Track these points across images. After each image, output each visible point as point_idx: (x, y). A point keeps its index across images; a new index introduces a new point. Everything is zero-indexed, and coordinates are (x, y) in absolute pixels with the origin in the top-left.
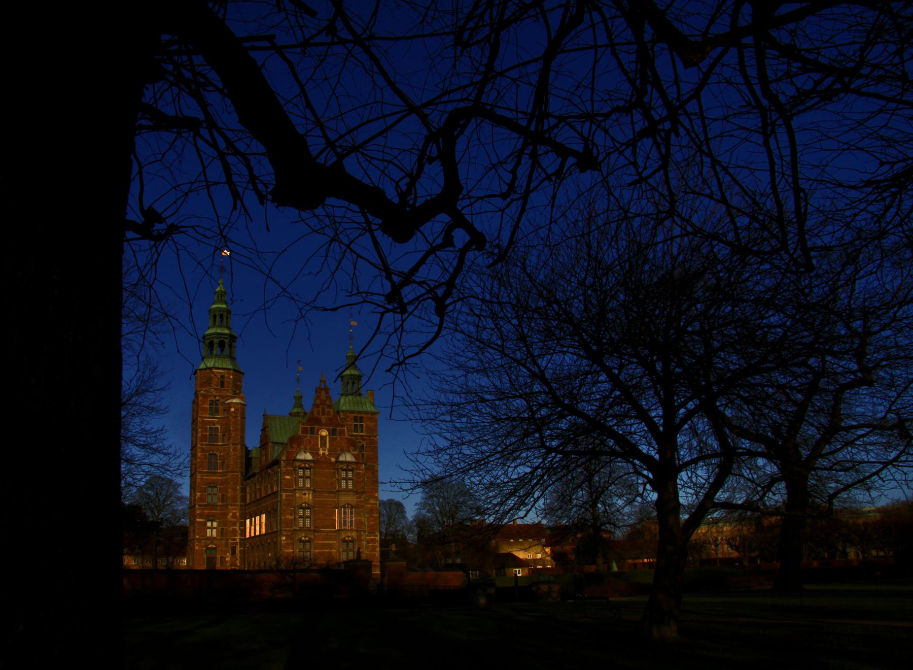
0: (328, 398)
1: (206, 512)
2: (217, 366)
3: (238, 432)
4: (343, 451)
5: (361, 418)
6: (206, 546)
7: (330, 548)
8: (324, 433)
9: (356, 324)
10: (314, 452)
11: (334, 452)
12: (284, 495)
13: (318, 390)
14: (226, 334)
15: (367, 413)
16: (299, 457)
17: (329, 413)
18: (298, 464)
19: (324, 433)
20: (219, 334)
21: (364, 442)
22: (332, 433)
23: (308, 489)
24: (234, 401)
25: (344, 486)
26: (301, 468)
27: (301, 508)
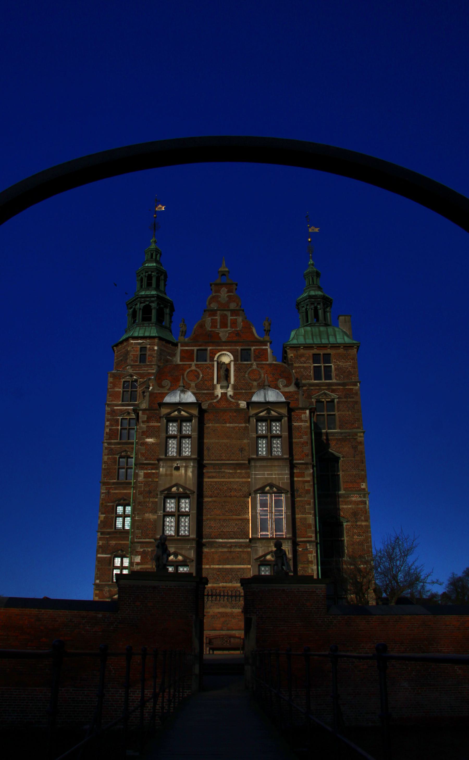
1: (113, 543)
2: (136, 334)
4: (262, 386)
8: (227, 358)
9: (317, 230)
10: (203, 390)
11: (244, 389)
12: (141, 473)
14: (153, 296)
15: (335, 346)
16: (168, 399)
17: (234, 323)
18: (164, 411)
19: (227, 358)
21: (334, 395)
22: (242, 357)
23: (186, 459)
25: (263, 451)
26: (174, 420)
27: (170, 496)
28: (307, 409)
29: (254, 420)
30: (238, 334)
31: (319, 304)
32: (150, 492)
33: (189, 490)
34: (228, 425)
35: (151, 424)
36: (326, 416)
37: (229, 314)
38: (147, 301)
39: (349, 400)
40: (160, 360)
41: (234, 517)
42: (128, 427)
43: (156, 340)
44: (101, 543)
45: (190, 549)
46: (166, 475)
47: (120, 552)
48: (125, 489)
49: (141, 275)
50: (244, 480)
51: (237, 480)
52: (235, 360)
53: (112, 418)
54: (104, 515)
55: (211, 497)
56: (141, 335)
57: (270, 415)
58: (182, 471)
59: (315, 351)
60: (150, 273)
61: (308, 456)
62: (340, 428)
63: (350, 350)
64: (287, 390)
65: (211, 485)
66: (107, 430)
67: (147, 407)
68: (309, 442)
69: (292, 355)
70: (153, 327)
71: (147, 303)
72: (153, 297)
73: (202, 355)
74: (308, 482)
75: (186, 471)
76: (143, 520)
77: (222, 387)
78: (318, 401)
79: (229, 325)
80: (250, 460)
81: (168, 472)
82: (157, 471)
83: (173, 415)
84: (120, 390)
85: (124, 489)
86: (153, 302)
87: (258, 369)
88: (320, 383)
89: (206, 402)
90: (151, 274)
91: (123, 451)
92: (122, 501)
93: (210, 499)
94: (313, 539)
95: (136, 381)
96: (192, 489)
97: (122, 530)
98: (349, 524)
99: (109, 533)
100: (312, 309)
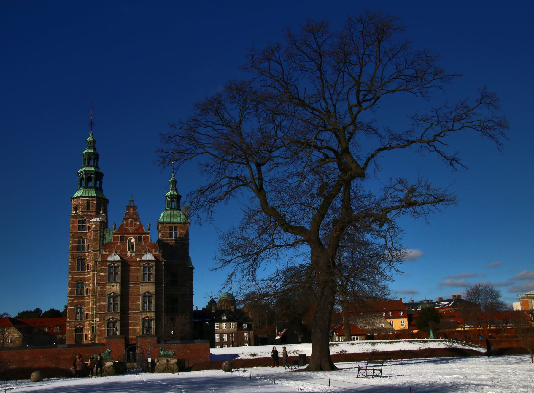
0: (135, 213)
1: (76, 301)
2: (84, 195)
3: (98, 242)
4: (146, 252)
5: (176, 227)
6: (75, 327)
7: (136, 326)
8: (133, 240)
12: (99, 287)
13: (129, 208)
14: (92, 171)
16: (110, 258)
17: (135, 224)
22: (139, 239)
24: (95, 219)
30: (137, 229)
32: (102, 294)
44: (69, 302)
48: (81, 275)
52: (136, 241)
56: (87, 195)
58: (115, 287)
59: (171, 225)
64: (155, 253)
66: (71, 246)
73: (122, 239)
95: (85, 220)
99: (73, 297)
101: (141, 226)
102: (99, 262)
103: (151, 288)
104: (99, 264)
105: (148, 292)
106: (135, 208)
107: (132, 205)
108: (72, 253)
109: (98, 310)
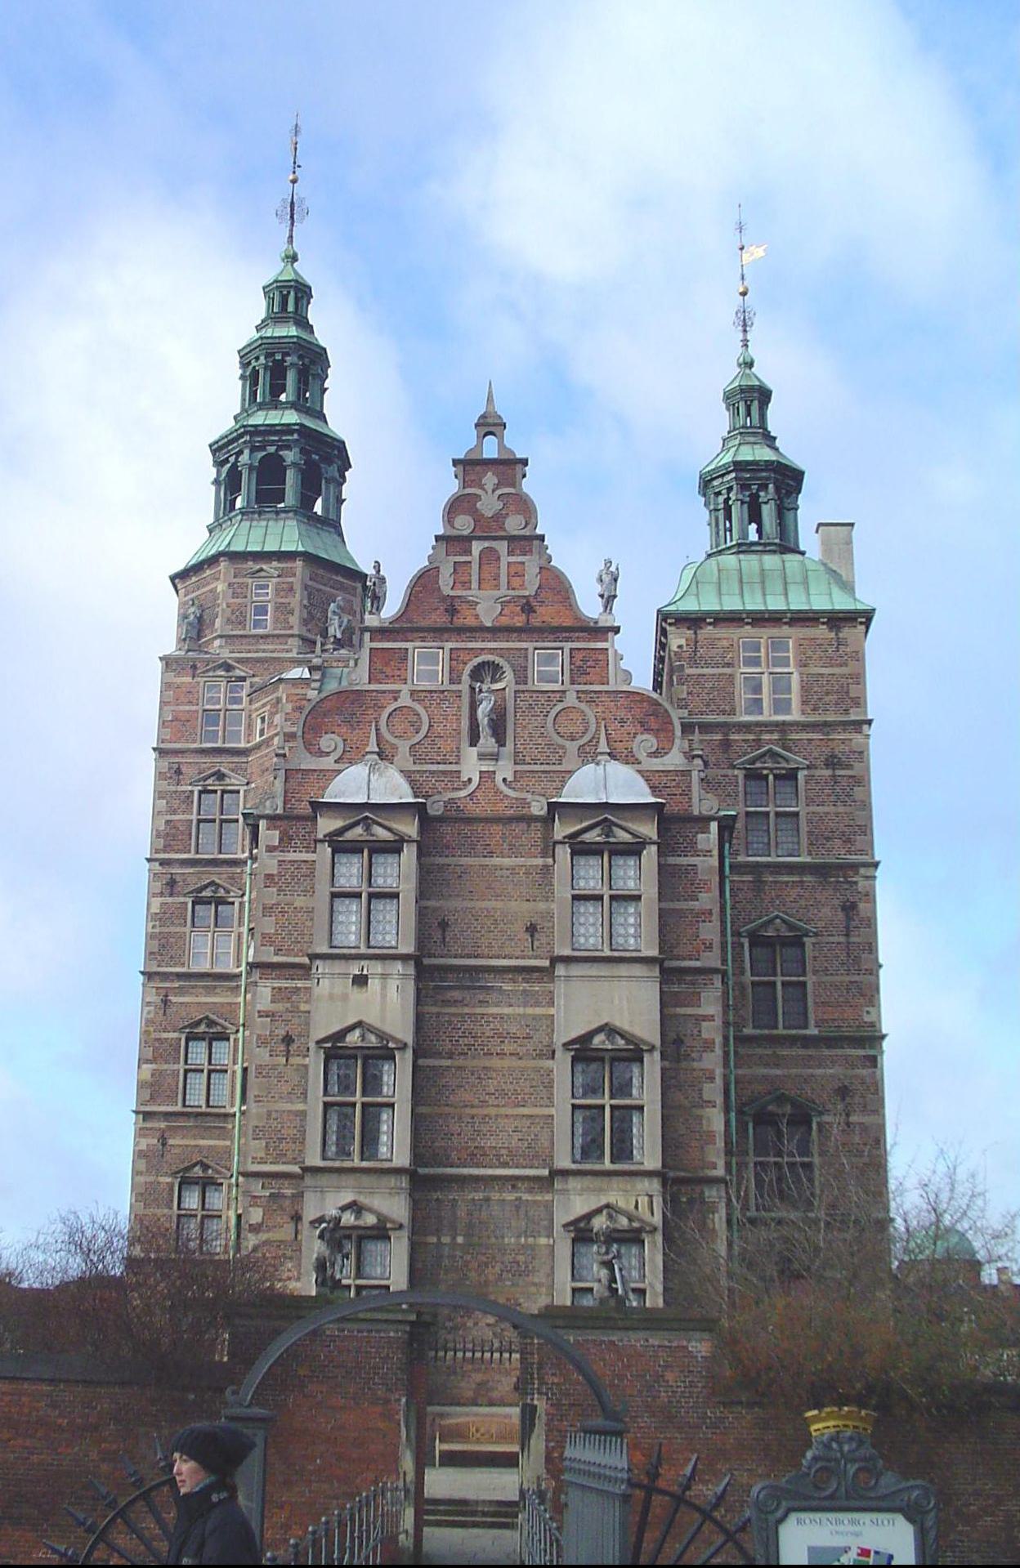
2: (238, 547)
4: (588, 755)
13: (469, 466)
14: (287, 429)
17: (517, 573)
18: (327, 825)
20: (255, 431)
26: (354, 848)
28: (713, 818)
29: (563, 853)
30: (528, 608)
31: (764, 487)
32: (288, 1040)
33: (394, 1039)
34: (496, 861)
35: (291, 856)
36: (772, 815)
37: (502, 547)
38: (272, 443)
39: (839, 772)
40: (305, 622)
41: (510, 1111)
42: (217, 817)
43: (299, 563)
45: (393, 1192)
46: (331, 997)
47: (197, 1169)
48: (210, 990)
49: (254, 363)
50: (538, 1011)
51: (521, 1010)
53: (173, 788)
54: (153, 1066)
55: (450, 1056)
57: (612, 840)
58: (374, 984)
60: (278, 357)
61: (710, 947)
62: (810, 853)
63: (846, 630)
64: (656, 764)
65: (450, 1022)
67: (280, 811)
68: (716, 910)
69: (683, 642)
70: (289, 523)
71: (272, 449)
72: (291, 432)
74: (711, 1018)
75: (384, 988)
76: (269, 1114)
77: (482, 757)
78: (753, 776)
79: (504, 579)
80: (555, 960)
81: (338, 990)
82: (307, 984)
83: (349, 835)
84: (194, 708)
85: (208, 994)
86: (288, 448)
87: (583, 706)
88: (758, 724)
89: (436, 798)
90: (283, 361)
91: (206, 887)
92: (202, 1028)
93: (448, 1063)
94: (720, 1172)
96: (399, 1036)
97: (204, 1109)
98: (826, 1118)
99: (167, 1115)
100: (743, 503)
101: (557, 586)
102: (272, 818)
103: (633, 1005)
104: (269, 835)
105: (609, 1030)
106: (511, 467)
107: (490, 449)
108: (163, 863)
109: (257, 1147)
